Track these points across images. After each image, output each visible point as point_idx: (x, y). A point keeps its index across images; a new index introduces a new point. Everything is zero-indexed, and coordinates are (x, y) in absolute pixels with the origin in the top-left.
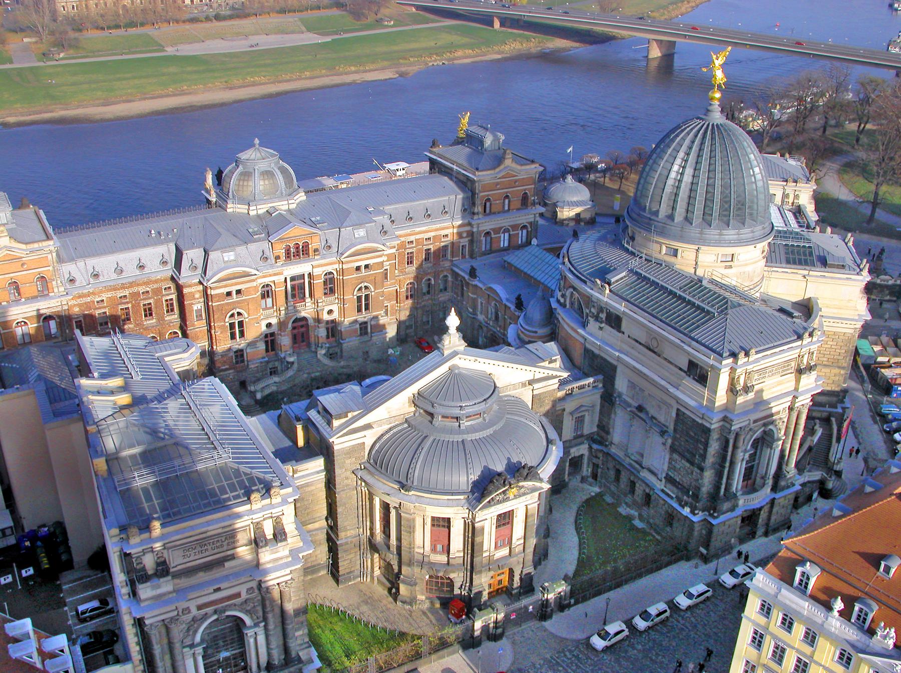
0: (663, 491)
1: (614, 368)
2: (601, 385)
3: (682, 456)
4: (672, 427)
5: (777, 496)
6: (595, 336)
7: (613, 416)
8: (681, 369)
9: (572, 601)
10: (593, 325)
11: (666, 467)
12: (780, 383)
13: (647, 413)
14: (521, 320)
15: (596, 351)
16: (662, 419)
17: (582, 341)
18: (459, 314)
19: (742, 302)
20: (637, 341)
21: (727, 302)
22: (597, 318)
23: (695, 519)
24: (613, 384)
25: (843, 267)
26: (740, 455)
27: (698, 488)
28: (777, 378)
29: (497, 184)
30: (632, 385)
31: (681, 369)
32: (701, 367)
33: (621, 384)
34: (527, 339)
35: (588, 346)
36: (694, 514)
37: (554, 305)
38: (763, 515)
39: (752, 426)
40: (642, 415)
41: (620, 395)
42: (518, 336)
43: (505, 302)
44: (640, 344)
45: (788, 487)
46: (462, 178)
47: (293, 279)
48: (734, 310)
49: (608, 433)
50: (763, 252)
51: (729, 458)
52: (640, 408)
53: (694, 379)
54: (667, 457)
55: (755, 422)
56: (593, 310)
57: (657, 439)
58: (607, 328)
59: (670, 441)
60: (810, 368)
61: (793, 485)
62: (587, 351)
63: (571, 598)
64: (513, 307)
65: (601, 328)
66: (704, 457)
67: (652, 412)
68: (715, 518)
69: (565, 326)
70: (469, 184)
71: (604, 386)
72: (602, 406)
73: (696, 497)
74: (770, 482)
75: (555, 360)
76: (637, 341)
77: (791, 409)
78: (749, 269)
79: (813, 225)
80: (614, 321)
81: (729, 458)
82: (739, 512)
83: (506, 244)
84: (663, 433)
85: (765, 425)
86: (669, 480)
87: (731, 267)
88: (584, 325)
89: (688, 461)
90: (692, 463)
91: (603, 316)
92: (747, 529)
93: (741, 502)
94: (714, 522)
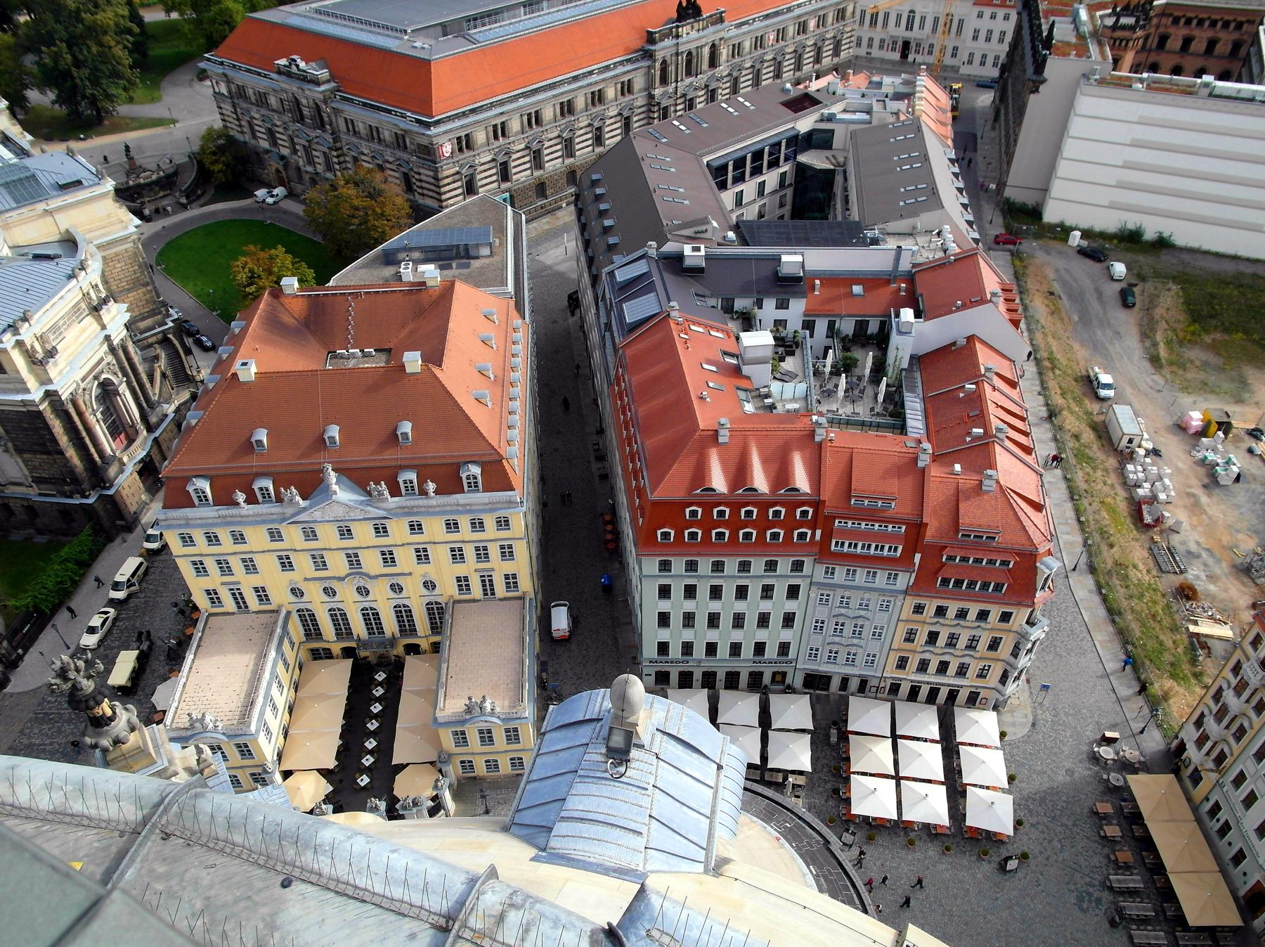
0: (40, 495)
3: (35, 452)
5: (157, 434)
9: (20, 651)
11: (27, 473)
12: (84, 330)
23: (91, 501)
26: (91, 419)
27: (71, 471)
28: (76, 328)
36: (87, 497)
38: (157, 458)
39: (82, 385)
45: (162, 421)
51: (81, 427)
54: (19, 460)
55: (83, 380)
59: (10, 445)
60: (105, 301)
61: (166, 416)
63: (15, 649)
66: (54, 440)
68: (109, 488)
73: (75, 480)
74: (141, 427)
77: (112, 350)
81: (81, 427)
82: (131, 467)
85: (96, 378)
86: (38, 481)
89: (42, 453)
90: (48, 453)
92: (150, 481)
93: (125, 459)
94: (111, 492)
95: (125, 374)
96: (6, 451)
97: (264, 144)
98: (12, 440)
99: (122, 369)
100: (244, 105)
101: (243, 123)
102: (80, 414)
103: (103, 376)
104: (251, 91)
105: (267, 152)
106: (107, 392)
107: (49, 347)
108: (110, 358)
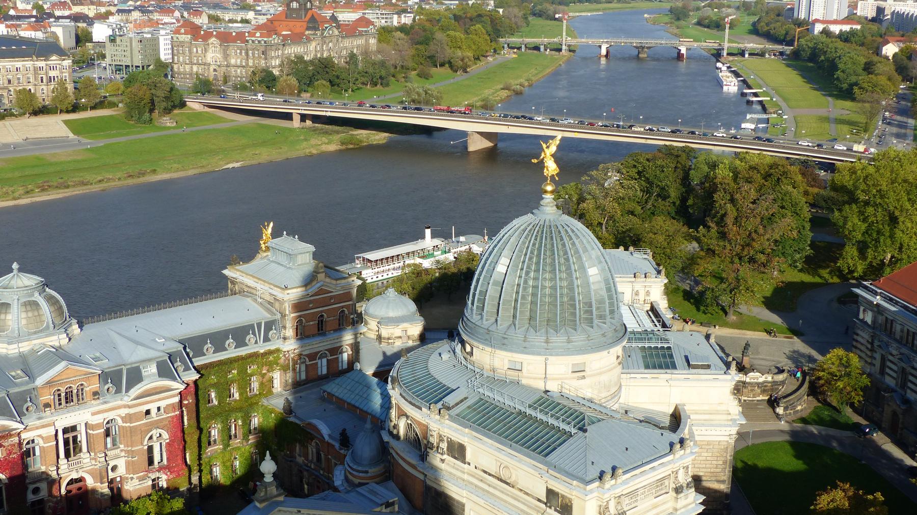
8: (539, 500)
14: (347, 458)
17: (422, 477)
18: (274, 458)
20: (485, 472)
21: (584, 419)
25: (708, 367)
29: (310, 302)
31: (539, 500)
32: (563, 496)
34: (357, 481)
35: (428, 482)
37: (386, 438)
42: (346, 479)
43: (327, 438)
44: (490, 475)
46: (268, 298)
47: (65, 431)
50: (618, 357)
53: (556, 510)
64: (337, 445)
69: (401, 462)
70: (277, 305)
75: (393, 504)
76: (485, 472)
78: (604, 378)
79: (668, 323)
83: (325, 371)
87: (584, 377)
91: (444, 446)
97: (890, 381)
100: (885, 339)
101: (875, 355)
104: (898, 328)
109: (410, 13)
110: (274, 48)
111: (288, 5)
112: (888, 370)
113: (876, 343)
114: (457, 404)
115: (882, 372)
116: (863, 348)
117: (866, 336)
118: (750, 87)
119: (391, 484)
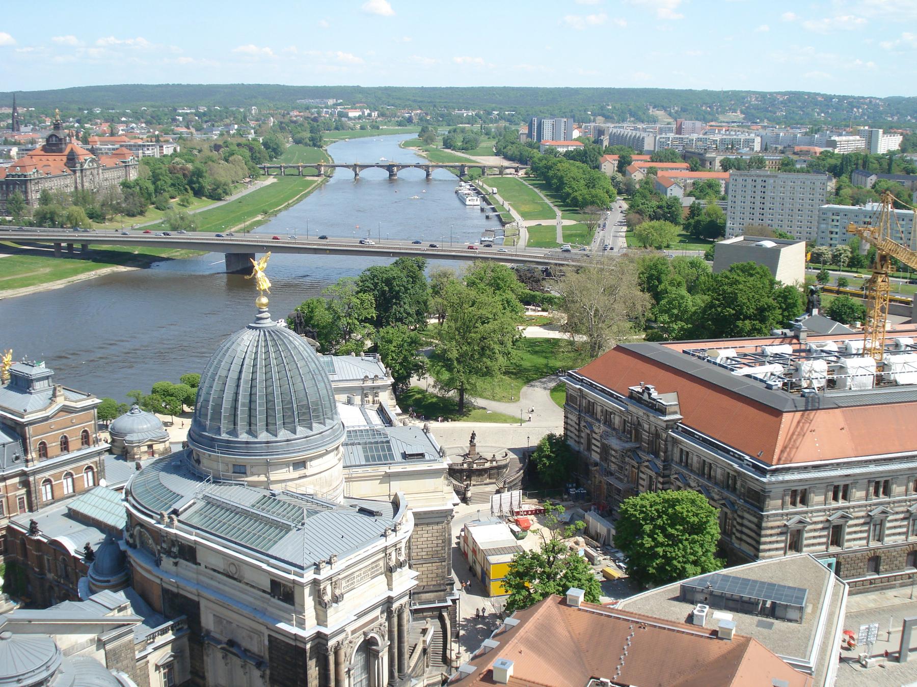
1: (198, 603)
2: (186, 627)
4: (267, 656)
6: (171, 575)
7: (205, 658)
10: (167, 562)
13: (239, 646)
15: (175, 590)
16: (255, 648)
17: (158, 581)
19: (319, 508)
20: (215, 570)
22: (169, 553)
24: (199, 623)
30: (218, 619)
33: (208, 621)
35: (165, 585)
40: (234, 650)
41: (208, 632)
44: (219, 572)
48: (311, 519)
49: (203, 678)
51: (332, 676)
52: (232, 643)
56: (164, 545)
57: (257, 673)
58: (182, 561)
59: (268, 672)
60: (401, 565)
62: (165, 592)
65: (176, 564)
67: (245, 644)
71: (189, 627)
72: (192, 650)
76: (215, 570)
80: (188, 552)
81: (332, 676)
84: (259, 665)
88: (158, 563)
91: (175, 550)
95: (391, 638)
96: (262, 677)
97: (596, 457)
98: (272, 669)
99: (390, 632)
100: (589, 419)
101: (583, 435)
102: (337, 664)
103: (371, 635)
104: (599, 409)
105: (596, 464)
106: (368, 648)
107: (338, 592)
108: (383, 619)
109: (171, 143)
110: (33, 182)
111: (48, 140)
112: (593, 447)
113: (583, 424)
114: (186, 510)
115: (589, 449)
116: (573, 429)
117: (575, 419)
118: (489, 204)
119: (130, 589)
